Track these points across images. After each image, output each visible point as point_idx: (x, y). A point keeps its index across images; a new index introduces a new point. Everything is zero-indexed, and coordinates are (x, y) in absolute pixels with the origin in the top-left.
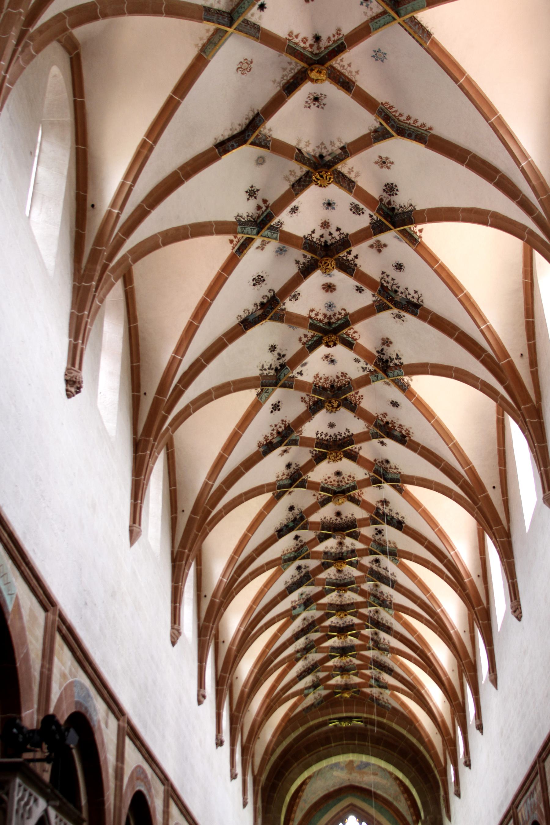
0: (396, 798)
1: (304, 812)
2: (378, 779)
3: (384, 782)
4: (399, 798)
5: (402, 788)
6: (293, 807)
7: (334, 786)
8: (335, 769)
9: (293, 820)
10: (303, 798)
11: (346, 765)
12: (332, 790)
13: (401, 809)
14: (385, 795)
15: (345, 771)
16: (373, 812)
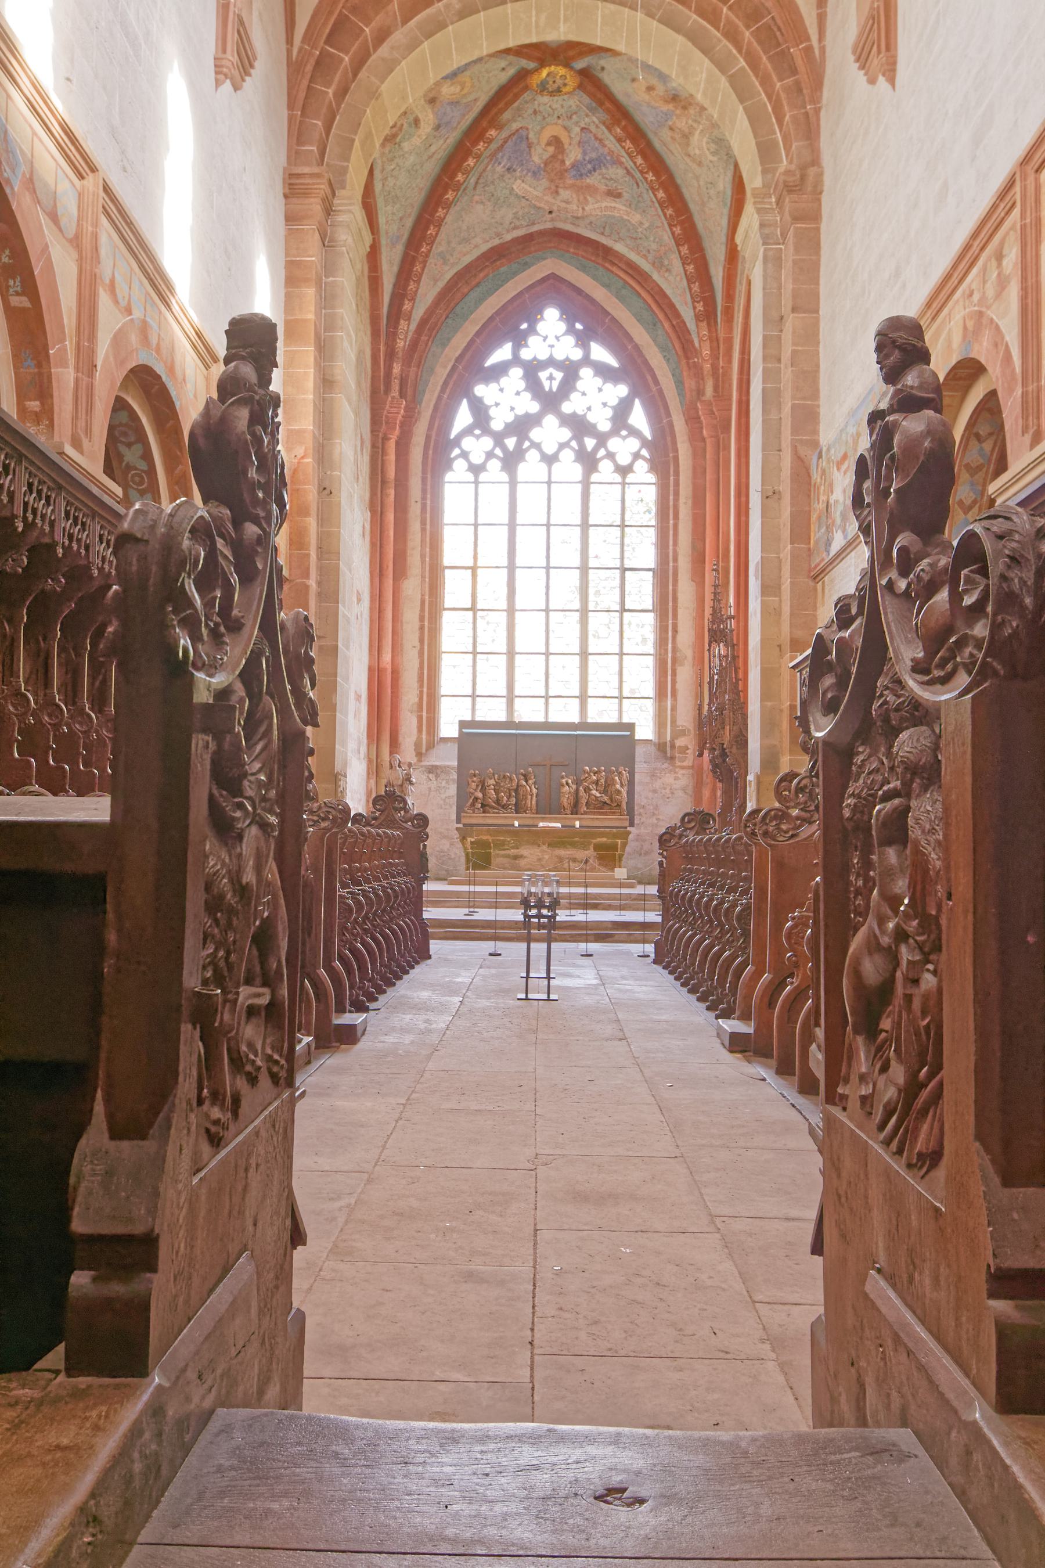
0: (659, 264)
1: (441, 285)
2: (619, 208)
3: (636, 218)
4: (666, 263)
5: (678, 230)
6: (412, 264)
7: (516, 228)
8: (518, 174)
9: (413, 300)
10: (437, 249)
11: (546, 164)
12: (508, 237)
13: (668, 292)
14: (633, 257)
15: (545, 183)
16: (599, 294)
